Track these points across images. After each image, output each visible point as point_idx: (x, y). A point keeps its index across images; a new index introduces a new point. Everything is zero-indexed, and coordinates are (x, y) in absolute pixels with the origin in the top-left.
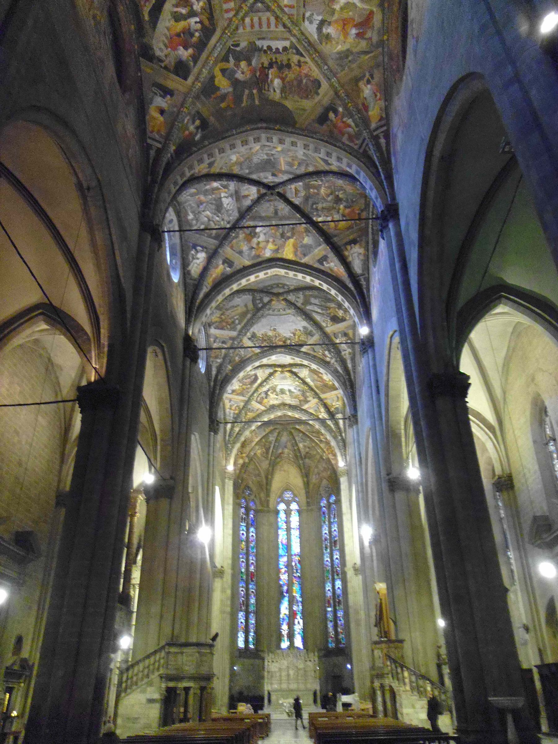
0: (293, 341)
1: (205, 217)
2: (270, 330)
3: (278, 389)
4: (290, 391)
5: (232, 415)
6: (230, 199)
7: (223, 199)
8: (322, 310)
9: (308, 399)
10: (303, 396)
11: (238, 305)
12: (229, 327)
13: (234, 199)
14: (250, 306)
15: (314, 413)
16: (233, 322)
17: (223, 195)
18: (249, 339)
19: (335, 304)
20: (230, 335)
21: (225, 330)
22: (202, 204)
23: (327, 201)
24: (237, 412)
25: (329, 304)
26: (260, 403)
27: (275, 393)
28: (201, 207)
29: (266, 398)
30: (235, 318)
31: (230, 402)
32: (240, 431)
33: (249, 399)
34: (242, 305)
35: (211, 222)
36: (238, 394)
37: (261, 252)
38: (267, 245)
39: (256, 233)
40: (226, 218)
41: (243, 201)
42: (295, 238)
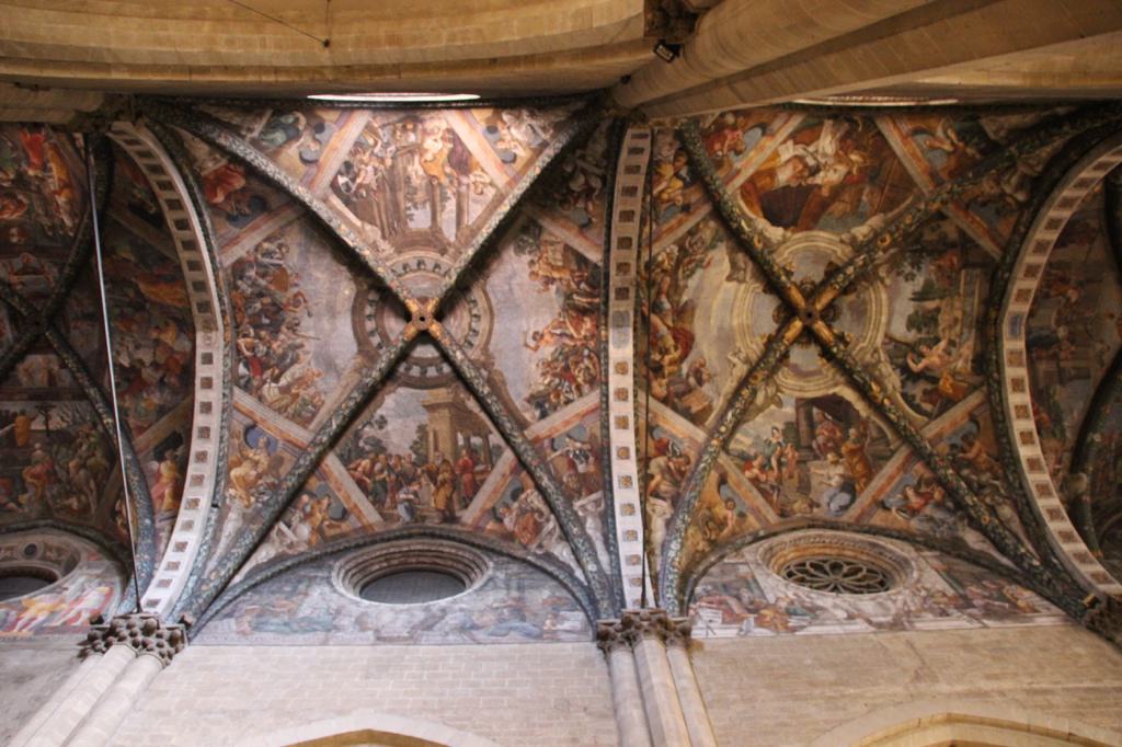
0: (573, 286)
1: (77, 472)
2: (536, 349)
3: (912, 336)
4: (920, 297)
5: (939, 515)
6: (53, 413)
7: (52, 426)
8: (444, 198)
9: (953, 236)
10: (941, 253)
11: (422, 429)
12: (479, 468)
13: (54, 403)
14: (442, 395)
15: (1012, 220)
16: (472, 451)
17: (37, 425)
18: (544, 415)
19: (411, 161)
20: (507, 470)
21: (483, 481)
22: (55, 473)
23: (31, 205)
24: (937, 495)
25: (416, 181)
26: (947, 403)
27: (924, 349)
28: (60, 475)
29: (935, 380)
30: (461, 442)
31: (887, 509)
32: (1015, 506)
33: (905, 437)
34: (425, 418)
35: (91, 461)
36: (869, 476)
37: (177, 361)
38: (166, 344)
39: (132, 367)
40: (86, 428)
41: (60, 384)
42: (133, 280)
